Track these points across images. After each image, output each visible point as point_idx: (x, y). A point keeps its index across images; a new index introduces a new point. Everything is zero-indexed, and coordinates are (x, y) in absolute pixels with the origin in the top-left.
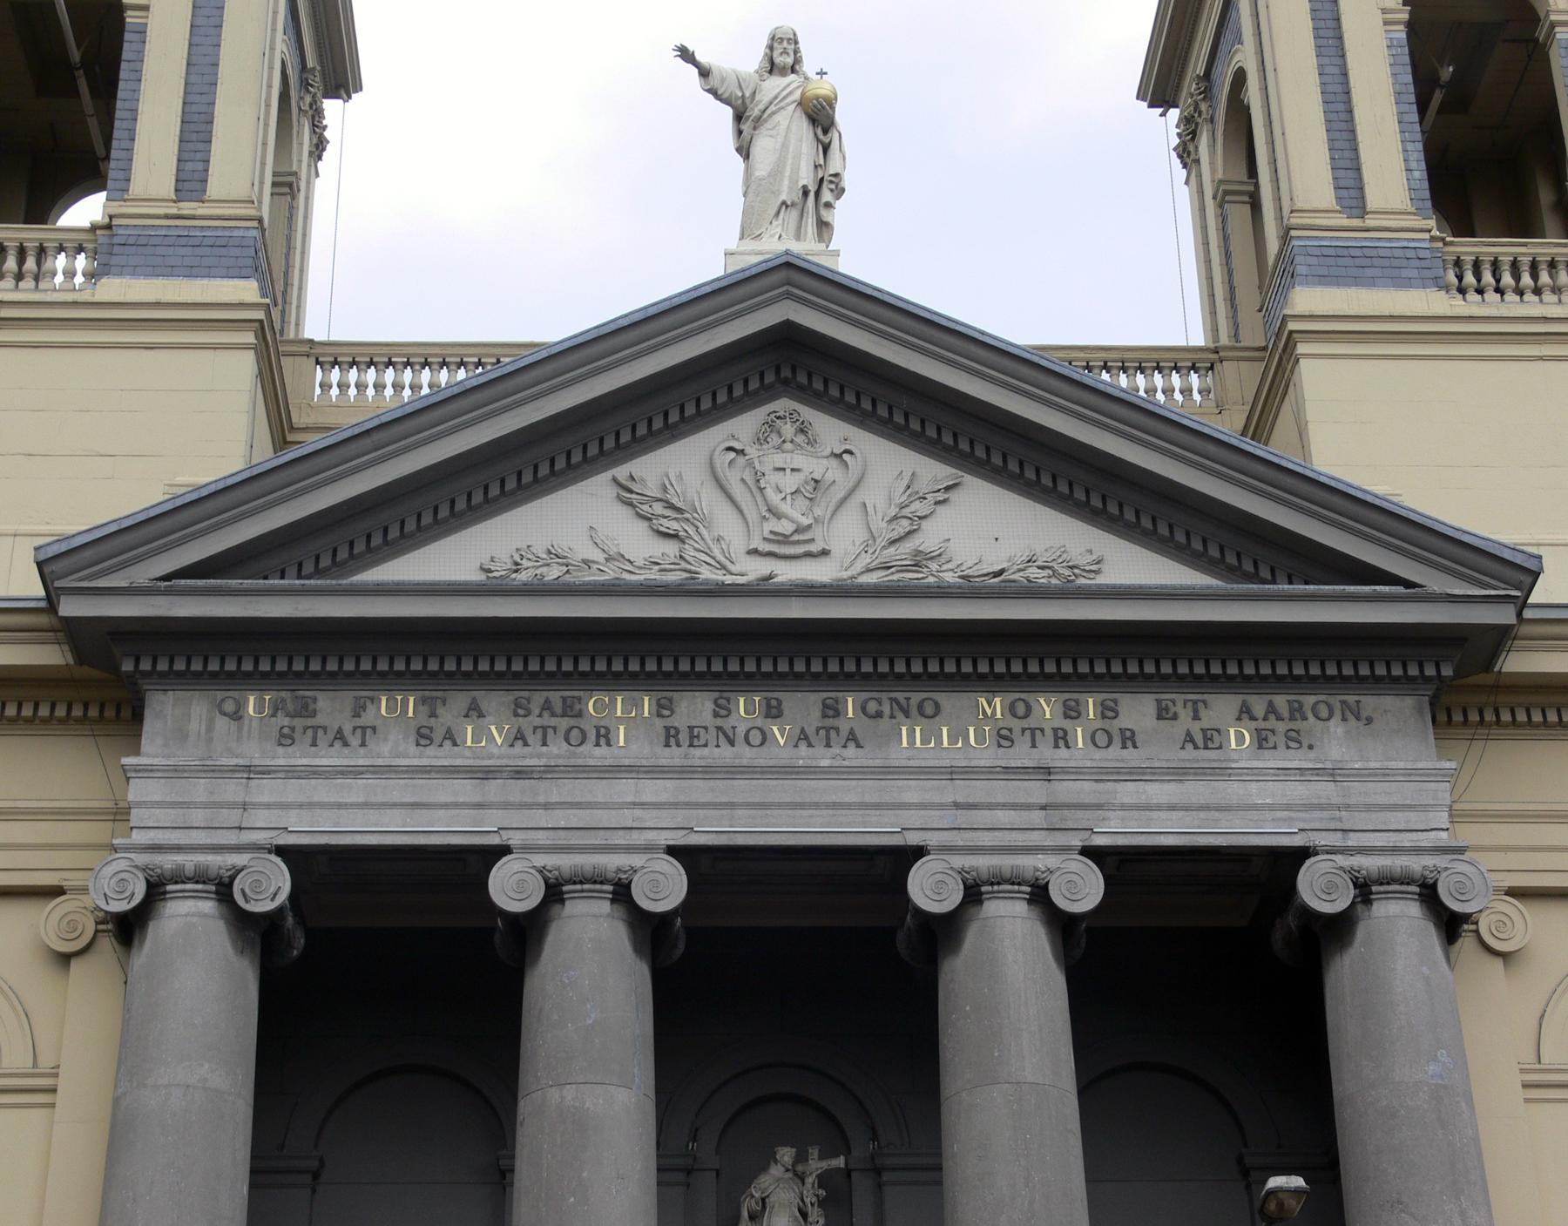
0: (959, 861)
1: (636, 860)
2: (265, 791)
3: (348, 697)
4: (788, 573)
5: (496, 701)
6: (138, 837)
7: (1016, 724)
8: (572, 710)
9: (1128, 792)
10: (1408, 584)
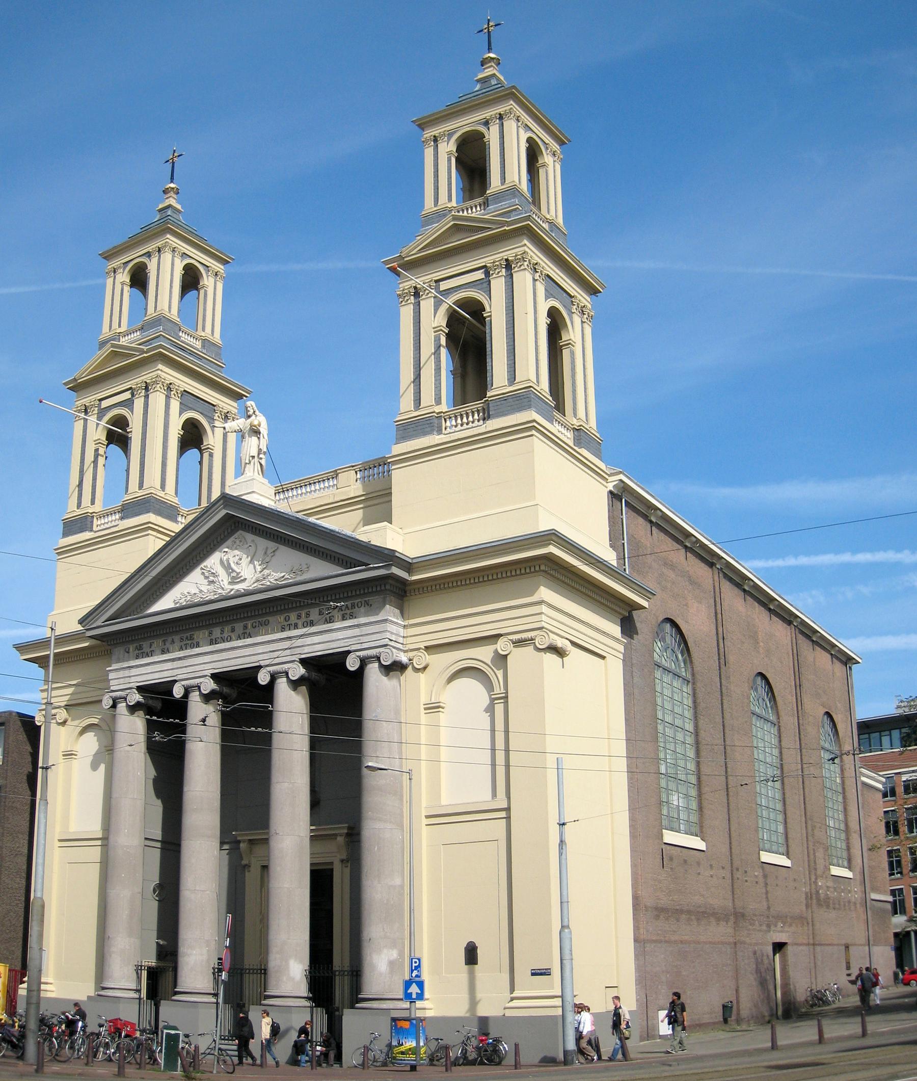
0: (271, 669)
1: (201, 680)
2: (134, 672)
5: (177, 638)
6: (112, 688)
8: (191, 638)
9: (309, 640)
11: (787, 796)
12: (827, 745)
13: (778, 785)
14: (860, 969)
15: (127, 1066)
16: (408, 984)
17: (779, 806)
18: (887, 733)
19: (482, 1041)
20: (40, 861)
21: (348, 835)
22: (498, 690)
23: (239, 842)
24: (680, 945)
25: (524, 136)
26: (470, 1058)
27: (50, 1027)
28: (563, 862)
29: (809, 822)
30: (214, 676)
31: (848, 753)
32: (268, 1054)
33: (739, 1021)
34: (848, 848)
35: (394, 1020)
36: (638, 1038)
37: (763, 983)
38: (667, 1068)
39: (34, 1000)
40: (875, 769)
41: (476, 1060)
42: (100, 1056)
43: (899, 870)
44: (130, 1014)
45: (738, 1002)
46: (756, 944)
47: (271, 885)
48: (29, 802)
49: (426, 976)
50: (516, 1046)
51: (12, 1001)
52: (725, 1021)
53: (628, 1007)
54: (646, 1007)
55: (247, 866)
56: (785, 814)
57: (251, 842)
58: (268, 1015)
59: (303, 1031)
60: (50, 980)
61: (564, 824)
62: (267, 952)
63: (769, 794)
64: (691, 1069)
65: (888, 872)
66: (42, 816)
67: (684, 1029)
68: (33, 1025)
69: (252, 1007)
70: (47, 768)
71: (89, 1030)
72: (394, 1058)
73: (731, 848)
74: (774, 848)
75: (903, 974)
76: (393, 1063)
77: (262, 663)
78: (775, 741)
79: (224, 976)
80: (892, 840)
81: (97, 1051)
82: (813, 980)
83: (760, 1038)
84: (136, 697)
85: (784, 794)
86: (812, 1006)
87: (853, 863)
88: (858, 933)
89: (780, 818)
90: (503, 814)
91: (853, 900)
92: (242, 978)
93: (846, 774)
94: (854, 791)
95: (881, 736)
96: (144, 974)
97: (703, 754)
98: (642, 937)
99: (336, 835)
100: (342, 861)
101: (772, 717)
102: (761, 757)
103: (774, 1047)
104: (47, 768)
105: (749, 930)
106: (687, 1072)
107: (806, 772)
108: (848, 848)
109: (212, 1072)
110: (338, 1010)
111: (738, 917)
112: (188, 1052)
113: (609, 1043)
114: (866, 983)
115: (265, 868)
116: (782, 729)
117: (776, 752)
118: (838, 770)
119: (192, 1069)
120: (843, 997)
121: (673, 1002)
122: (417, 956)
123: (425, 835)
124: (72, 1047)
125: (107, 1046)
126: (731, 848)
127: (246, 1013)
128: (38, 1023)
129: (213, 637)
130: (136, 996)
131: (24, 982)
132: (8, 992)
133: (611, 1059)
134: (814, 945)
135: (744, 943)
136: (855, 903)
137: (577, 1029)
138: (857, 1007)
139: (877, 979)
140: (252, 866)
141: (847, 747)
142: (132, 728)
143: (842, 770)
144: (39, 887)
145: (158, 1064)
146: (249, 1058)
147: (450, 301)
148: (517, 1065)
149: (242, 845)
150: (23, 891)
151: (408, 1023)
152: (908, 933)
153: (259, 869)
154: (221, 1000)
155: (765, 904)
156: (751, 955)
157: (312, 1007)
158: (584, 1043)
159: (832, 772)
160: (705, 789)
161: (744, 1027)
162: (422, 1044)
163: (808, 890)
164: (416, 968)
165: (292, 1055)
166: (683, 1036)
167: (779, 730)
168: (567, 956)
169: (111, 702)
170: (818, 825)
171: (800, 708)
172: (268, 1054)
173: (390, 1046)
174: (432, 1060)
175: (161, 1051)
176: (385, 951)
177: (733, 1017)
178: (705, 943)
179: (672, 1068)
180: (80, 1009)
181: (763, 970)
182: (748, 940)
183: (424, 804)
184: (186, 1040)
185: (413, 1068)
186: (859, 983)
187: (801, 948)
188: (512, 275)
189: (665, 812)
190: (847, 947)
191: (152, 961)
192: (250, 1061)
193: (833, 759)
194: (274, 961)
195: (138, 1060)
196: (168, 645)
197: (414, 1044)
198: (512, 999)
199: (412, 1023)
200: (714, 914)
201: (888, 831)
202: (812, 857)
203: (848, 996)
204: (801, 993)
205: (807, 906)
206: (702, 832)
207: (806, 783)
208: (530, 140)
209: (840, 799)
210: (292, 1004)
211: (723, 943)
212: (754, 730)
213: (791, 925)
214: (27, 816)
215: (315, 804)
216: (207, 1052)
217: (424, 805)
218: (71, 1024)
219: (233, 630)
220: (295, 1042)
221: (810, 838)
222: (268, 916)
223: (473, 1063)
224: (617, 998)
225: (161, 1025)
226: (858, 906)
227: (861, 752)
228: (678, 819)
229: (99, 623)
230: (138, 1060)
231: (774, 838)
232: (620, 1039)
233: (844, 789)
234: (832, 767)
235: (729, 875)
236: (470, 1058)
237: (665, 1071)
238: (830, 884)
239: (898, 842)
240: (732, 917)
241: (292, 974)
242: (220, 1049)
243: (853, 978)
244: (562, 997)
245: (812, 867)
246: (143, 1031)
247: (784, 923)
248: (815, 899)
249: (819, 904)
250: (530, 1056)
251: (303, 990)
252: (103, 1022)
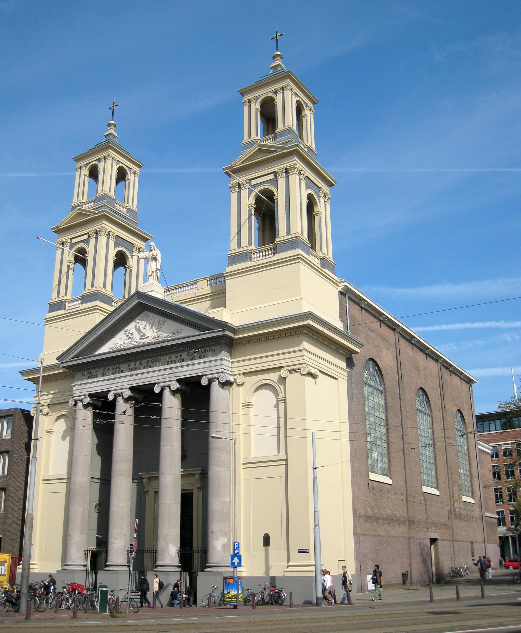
0: (161, 384)
2: (87, 386)
3: (95, 370)
4: (143, 341)
5: (110, 368)
6: (75, 395)
7: (169, 360)
8: (119, 368)
9: (182, 369)
11: (437, 455)
12: (459, 428)
13: (432, 449)
14: (480, 557)
15: (78, 611)
16: (233, 557)
17: (432, 461)
18: (493, 422)
19: (272, 590)
20: (31, 492)
21: (202, 474)
22: (281, 396)
23: (143, 478)
24: (379, 538)
25: (295, 99)
26: (266, 601)
27: (35, 591)
28: (316, 489)
29: (449, 470)
30: (131, 389)
31: (471, 433)
32: (157, 600)
33: (411, 584)
34: (472, 486)
35: (225, 578)
36: (356, 591)
37: (425, 562)
38: (372, 610)
39: (26, 575)
40: (487, 442)
41: (269, 602)
42: (63, 606)
43: (501, 500)
44: (80, 580)
45: (411, 572)
46: (421, 539)
47: (160, 502)
48: (26, 459)
49: (242, 553)
50: (291, 594)
51: (13, 576)
52: (404, 583)
53: (351, 572)
54: (360, 572)
55: (147, 492)
56: (436, 465)
57: (149, 478)
58: (157, 577)
59: (176, 586)
60: (35, 562)
61: (316, 468)
62: (157, 540)
63: (427, 454)
64: (386, 611)
65: (495, 501)
66: (33, 467)
67: (381, 587)
68: (25, 590)
69: (148, 572)
70: (36, 440)
71: (57, 591)
72: (225, 601)
73: (406, 484)
74: (430, 484)
75: (505, 561)
76: (224, 604)
77: (157, 381)
78: (430, 425)
79: (133, 555)
80: (497, 482)
81: (62, 603)
82: (453, 561)
83: (423, 595)
84: (88, 400)
85: (435, 454)
86: (453, 577)
87: (475, 494)
88: (478, 536)
89: (433, 467)
90: (284, 463)
91: (475, 516)
92: (143, 556)
93: (470, 444)
94: (475, 454)
95: (489, 424)
96: (89, 555)
97: (390, 431)
98: (358, 532)
99: (195, 474)
100: (198, 488)
101: (428, 412)
102: (422, 434)
103: (431, 600)
104: (36, 440)
105: (417, 530)
106: (383, 613)
107: (447, 443)
108: (472, 486)
109: (126, 613)
110: (195, 573)
111: (411, 522)
112: (113, 601)
113: (340, 594)
114: (484, 565)
115: (157, 492)
116: (434, 418)
117: (430, 431)
118: (465, 442)
119: (115, 611)
120: (470, 573)
121: (375, 571)
122: (238, 541)
123: (242, 474)
124: (47, 602)
125: (67, 600)
126: (406, 484)
127: (145, 576)
128: (28, 589)
129: (130, 367)
130: (84, 568)
131: (20, 564)
132: (11, 571)
133: (341, 603)
134: (453, 541)
135: (413, 538)
136: (476, 518)
137: (323, 584)
138: (478, 580)
139: (490, 564)
140: (150, 491)
141: (470, 429)
142: (85, 417)
143: (468, 442)
144: (30, 507)
145: (96, 609)
146: (147, 603)
147: (257, 190)
148: (291, 606)
149: (144, 480)
150: (21, 510)
151: (232, 580)
152: (507, 537)
153: (153, 493)
154: (131, 569)
155: (425, 516)
156: (418, 545)
157: (181, 572)
158: (327, 594)
159: (462, 443)
160: (392, 451)
161: (414, 587)
162: (240, 592)
163: (449, 509)
164: (237, 548)
165: (170, 601)
166: (381, 591)
167: (432, 419)
168: (317, 542)
169: (74, 403)
170: (454, 472)
171: (443, 407)
172: (157, 600)
173: (223, 594)
174: (245, 602)
175: (98, 601)
176: (221, 538)
177: (409, 581)
178: (393, 537)
179: (375, 610)
180: (52, 578)
181: (424, 554)
182: (416, 536)
183: (242, 457)
184: (112, 593)
185: (235, 607)
186: (479, 565)
187: (446, 542)
189: (370, 462)
190: (472, 543)
191: (94, 548)
192: (147, 605)
193: (462, 436)
194: (161, 545)
195: (85, 608)
196: (106, 371)
197: (236, 593)
198: (288, 566)
199: (234, 580)
200: (397, 520)
201: (494, 477)
202: (451, 490)
203: (473, 572)
204: (446, 570)
205: (449, 518)
206: (390, 474)
207: (448, 448)
208: (298, 102)
209: (467, 458)
210: (170, 570)
211: (402, 537)
212: (418, 419)
213: (440, 529)
214: (24, 467)
215: (184, 457)
216: (123, 600)
217: (242, 457)
218: (47, 588)
219: (141, 364)
220: (172, 592)
221: (450, 479)
222: (158, 520)
223: (267, 604)
224: (345, 567)
225: (98, 585)
226: (478, 519)
227: (478, 432)
228: (377, 466)
229: (68, 359)
230: (85, 608)
231: (430, 479)
232: (346, 591)
233: (469, 452)
234: (462, 440)
235: (405, 499)
236: (266, 601)
237: (371, 612)
238: (462, 506)
239: (500, 484)
240: (407, 523)
241: (170, 553)
242: (130, 598)
243: (476, 562)
244: (315, 565)
245: (451, 496)
246: (88, 590)
247: (436, 527)
248: (453, 515)
249: (456, 518)
250: (298, 600)
251: (176, 561)
252: (65, 585)
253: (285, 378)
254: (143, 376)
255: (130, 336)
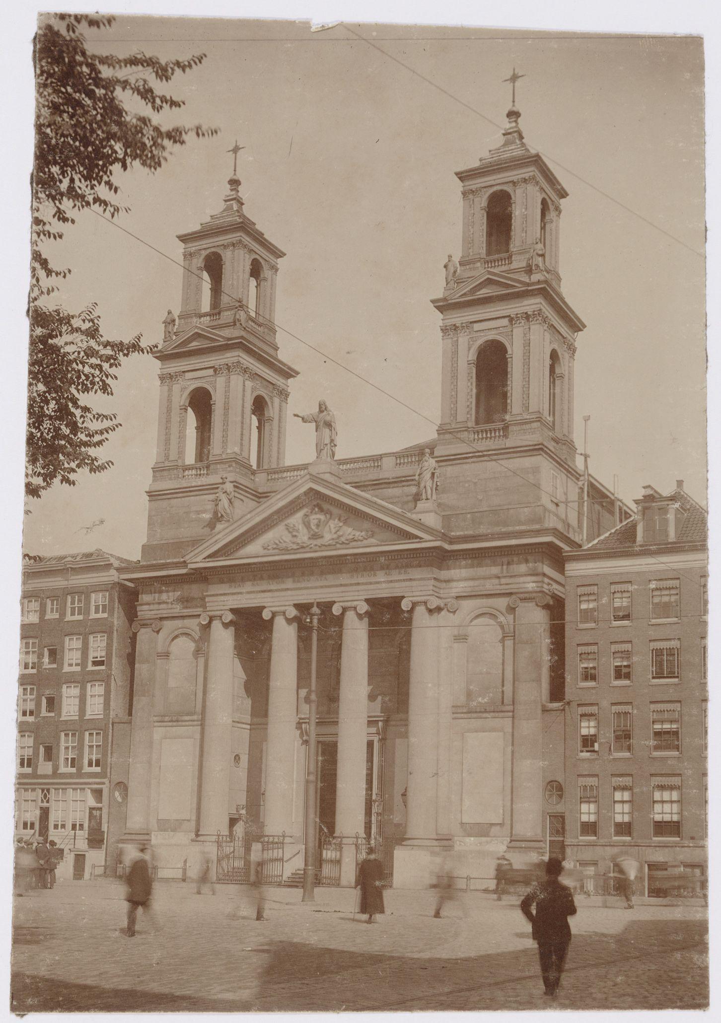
1: (287, 608)
10: (421, 538)
77: (336, 600)
188: (554, 380)
229: (198, 559)
253: (514, 609)
254: (314, 591)
255: (294, 533)
